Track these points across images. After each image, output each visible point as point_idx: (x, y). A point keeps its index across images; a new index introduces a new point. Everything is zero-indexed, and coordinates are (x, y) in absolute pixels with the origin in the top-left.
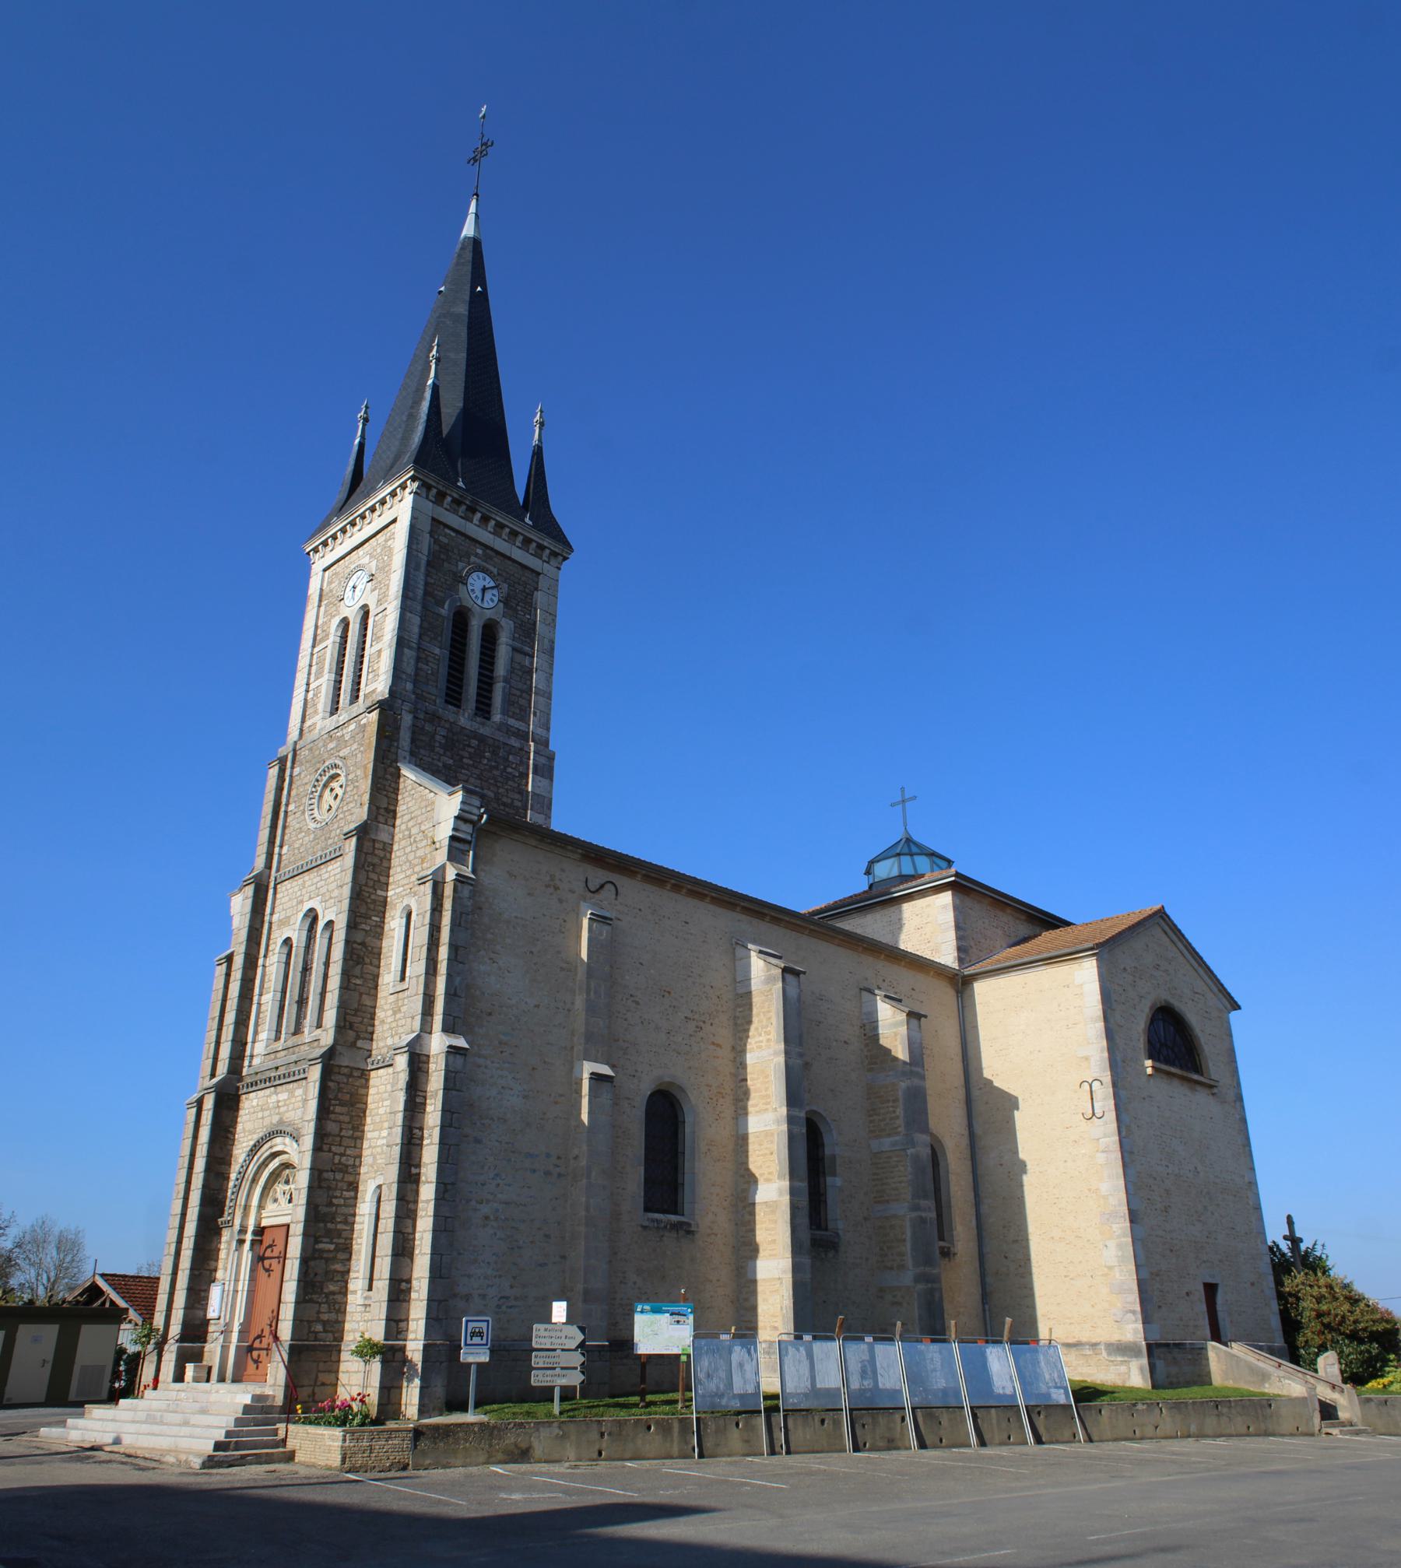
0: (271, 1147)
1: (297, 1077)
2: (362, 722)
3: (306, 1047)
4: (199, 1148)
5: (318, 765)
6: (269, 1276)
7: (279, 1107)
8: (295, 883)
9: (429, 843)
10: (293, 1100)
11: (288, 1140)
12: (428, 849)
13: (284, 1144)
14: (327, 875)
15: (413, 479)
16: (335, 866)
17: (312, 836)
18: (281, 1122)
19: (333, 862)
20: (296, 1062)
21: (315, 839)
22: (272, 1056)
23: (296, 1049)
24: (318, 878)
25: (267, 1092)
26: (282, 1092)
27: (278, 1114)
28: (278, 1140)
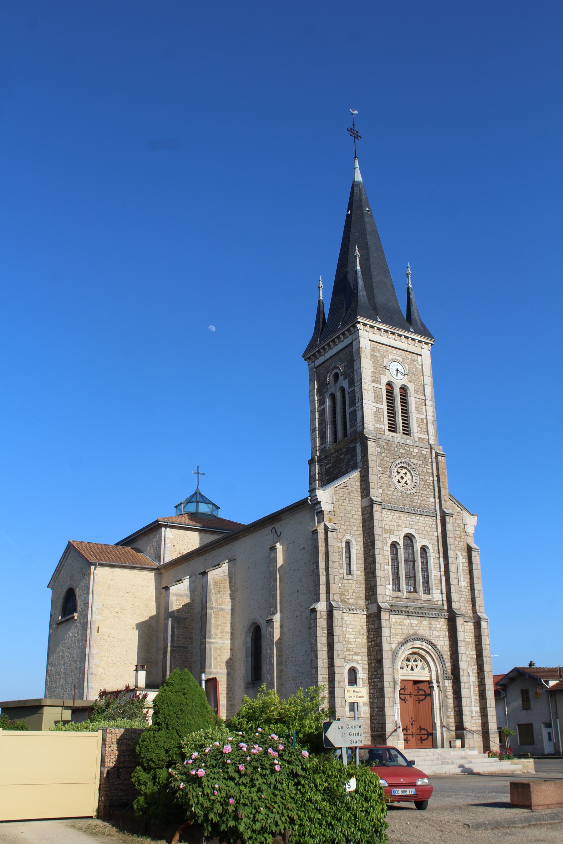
0: (412, 645)
1: (424, 615)
2: (423, 452)
3: (422, 601)
4: (462, 649)
5: (395, 457)
6: (405, 702)
7: (412, 626)
8: (392, 514)
9: (462, 530)
10: (422, 625)
11: (424, 643)
12: (462, 533)
13: (422, 645)
14: (417, 521)
15: (432, 345)
16: (421, 518)
17: (400, 494)
18: (415, 634)
19: (419, 516)
20: (420, 608)
21: (402, 496)
22: (399, 599)
23: (416, 601)
24: (411, 520)
25: (403, 617)
26: (413, 619)
27: (413, 629)
28: (418, 642)
